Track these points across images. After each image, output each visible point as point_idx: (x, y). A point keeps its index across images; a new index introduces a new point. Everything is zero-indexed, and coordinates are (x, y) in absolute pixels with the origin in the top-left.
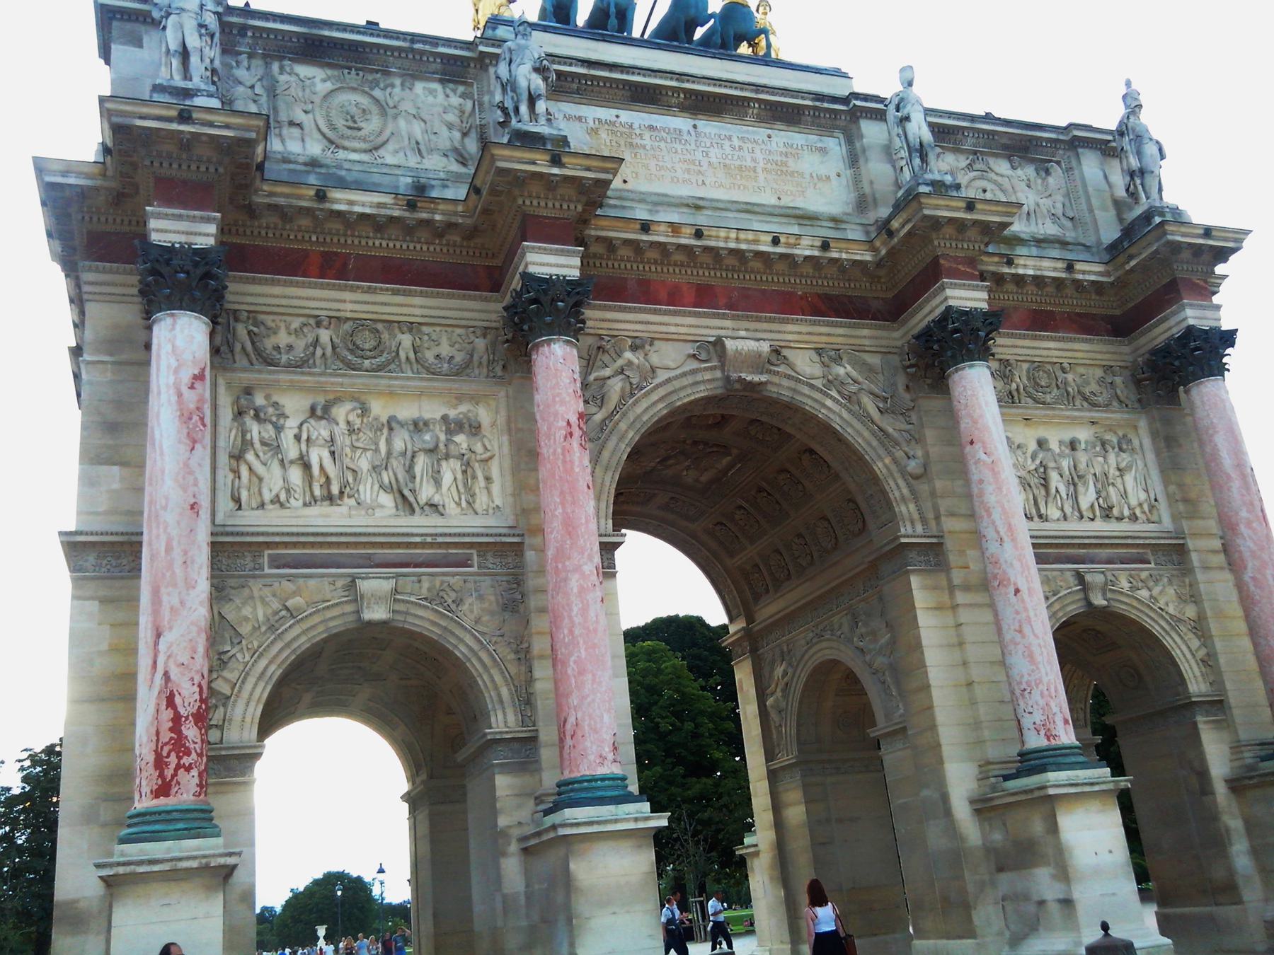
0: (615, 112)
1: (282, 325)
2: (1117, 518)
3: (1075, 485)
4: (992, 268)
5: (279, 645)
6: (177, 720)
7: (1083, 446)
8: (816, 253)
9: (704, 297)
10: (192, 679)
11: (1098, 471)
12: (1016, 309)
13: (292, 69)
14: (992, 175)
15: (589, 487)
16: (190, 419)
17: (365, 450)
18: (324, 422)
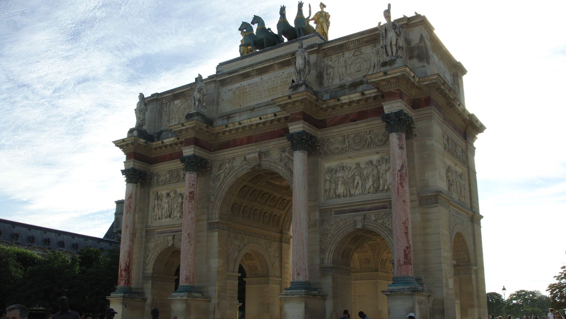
0: (241, 83)
1: (162, 175)
2: (381, 191)
3: (366, 180)
4: (332, 104)
5: (156, 252)
6: (121, 270)
7: (374, 163)
8: (273, 118)
9: (249, 140)
10: (124, 262)
11: (375, 172)
13: (174, 103)
15: (189, 212)
16: (127, 207)
17: (175, 203)
18: (168, 197)
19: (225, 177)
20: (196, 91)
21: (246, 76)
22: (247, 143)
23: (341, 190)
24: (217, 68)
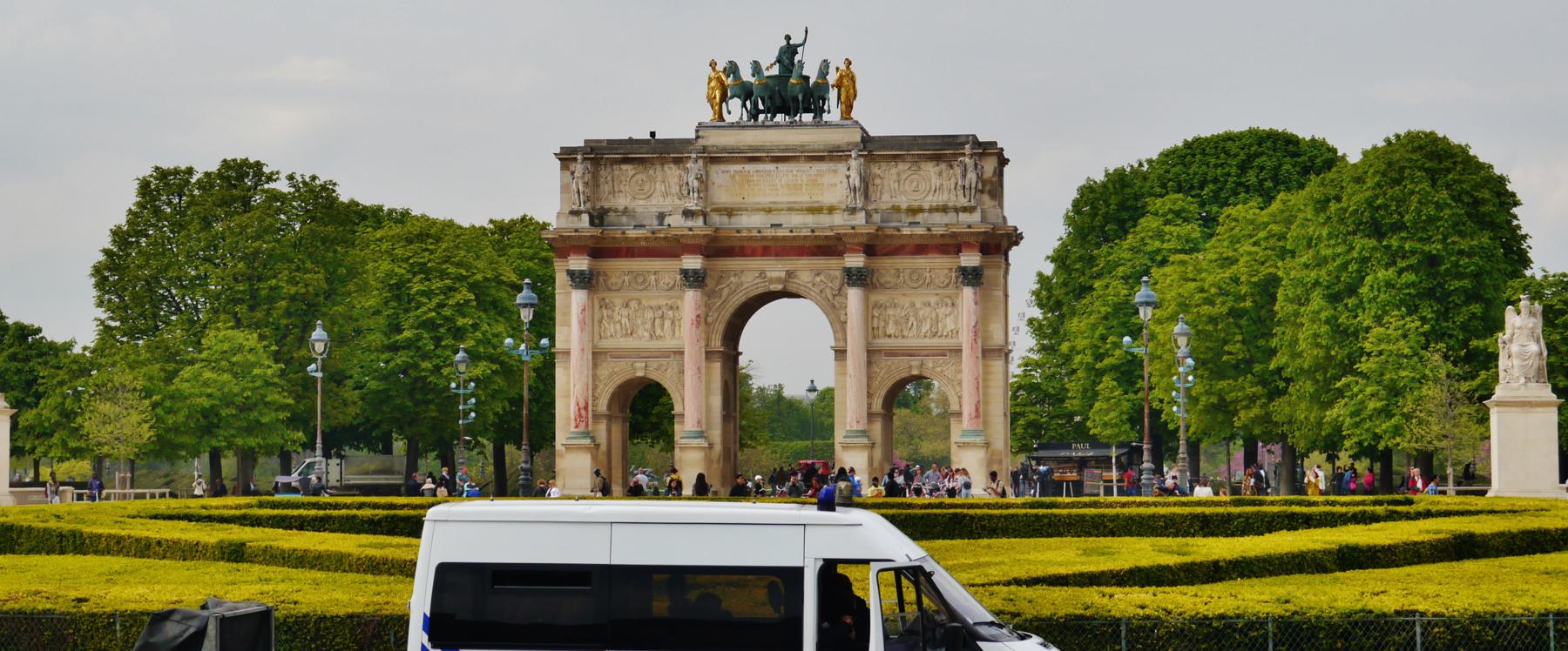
11: (934, 315)
12: (908, 245)
14: (921, 173)
19: (729, 294)
20: (693, 177)
21: (753, 157)
22: (762, 256)
23: (891, 329)
24: (697, 131)
